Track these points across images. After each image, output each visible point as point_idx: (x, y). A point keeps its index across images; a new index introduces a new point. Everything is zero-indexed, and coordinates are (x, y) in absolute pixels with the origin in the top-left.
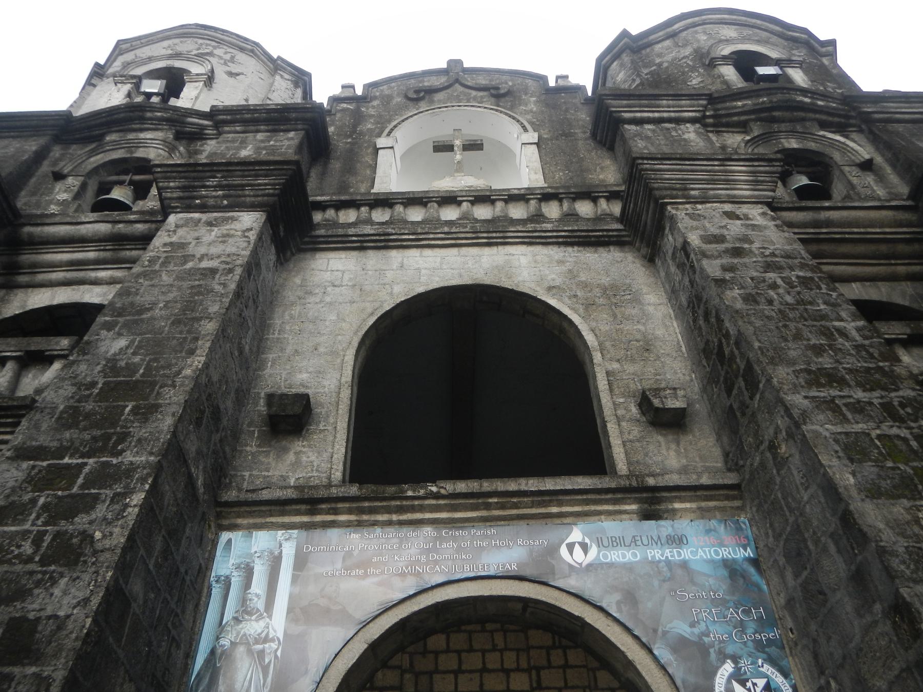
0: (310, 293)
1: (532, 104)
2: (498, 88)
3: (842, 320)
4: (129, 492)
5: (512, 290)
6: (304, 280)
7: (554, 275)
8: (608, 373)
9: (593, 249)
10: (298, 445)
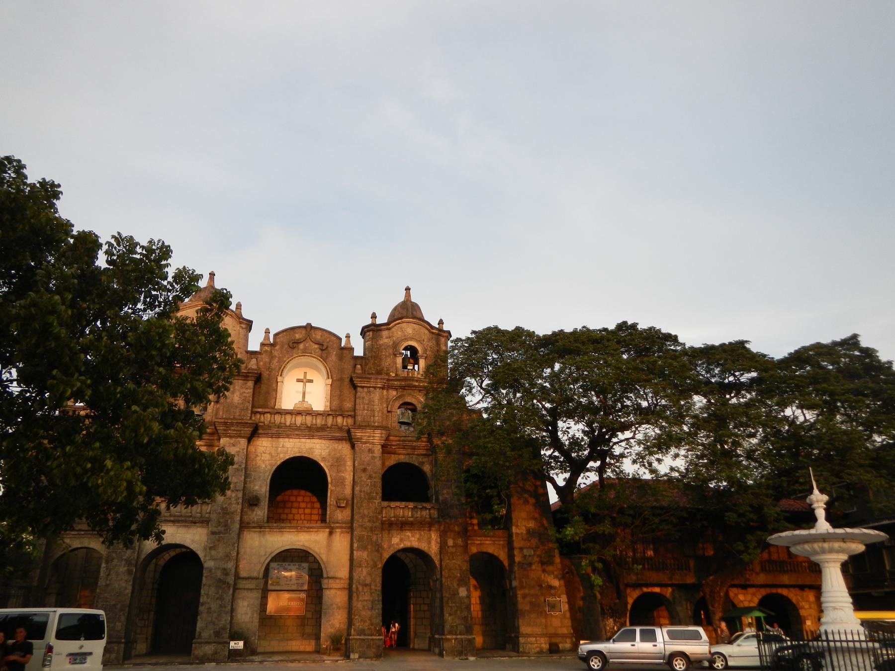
0: (257, 455)
1: (333, 357)
2: (322, 345)
3: (376, 499)
4: (235, 544)
5: (312, 459)
6: (255, 450)
7: (325, 453)
8: (331, 491)
9: (337, 441)
10: (256, 508)
